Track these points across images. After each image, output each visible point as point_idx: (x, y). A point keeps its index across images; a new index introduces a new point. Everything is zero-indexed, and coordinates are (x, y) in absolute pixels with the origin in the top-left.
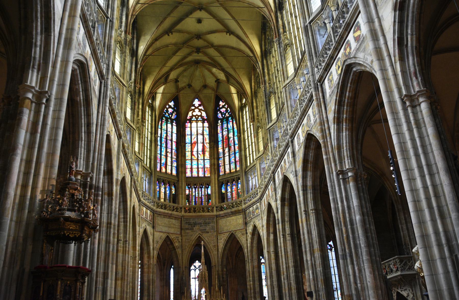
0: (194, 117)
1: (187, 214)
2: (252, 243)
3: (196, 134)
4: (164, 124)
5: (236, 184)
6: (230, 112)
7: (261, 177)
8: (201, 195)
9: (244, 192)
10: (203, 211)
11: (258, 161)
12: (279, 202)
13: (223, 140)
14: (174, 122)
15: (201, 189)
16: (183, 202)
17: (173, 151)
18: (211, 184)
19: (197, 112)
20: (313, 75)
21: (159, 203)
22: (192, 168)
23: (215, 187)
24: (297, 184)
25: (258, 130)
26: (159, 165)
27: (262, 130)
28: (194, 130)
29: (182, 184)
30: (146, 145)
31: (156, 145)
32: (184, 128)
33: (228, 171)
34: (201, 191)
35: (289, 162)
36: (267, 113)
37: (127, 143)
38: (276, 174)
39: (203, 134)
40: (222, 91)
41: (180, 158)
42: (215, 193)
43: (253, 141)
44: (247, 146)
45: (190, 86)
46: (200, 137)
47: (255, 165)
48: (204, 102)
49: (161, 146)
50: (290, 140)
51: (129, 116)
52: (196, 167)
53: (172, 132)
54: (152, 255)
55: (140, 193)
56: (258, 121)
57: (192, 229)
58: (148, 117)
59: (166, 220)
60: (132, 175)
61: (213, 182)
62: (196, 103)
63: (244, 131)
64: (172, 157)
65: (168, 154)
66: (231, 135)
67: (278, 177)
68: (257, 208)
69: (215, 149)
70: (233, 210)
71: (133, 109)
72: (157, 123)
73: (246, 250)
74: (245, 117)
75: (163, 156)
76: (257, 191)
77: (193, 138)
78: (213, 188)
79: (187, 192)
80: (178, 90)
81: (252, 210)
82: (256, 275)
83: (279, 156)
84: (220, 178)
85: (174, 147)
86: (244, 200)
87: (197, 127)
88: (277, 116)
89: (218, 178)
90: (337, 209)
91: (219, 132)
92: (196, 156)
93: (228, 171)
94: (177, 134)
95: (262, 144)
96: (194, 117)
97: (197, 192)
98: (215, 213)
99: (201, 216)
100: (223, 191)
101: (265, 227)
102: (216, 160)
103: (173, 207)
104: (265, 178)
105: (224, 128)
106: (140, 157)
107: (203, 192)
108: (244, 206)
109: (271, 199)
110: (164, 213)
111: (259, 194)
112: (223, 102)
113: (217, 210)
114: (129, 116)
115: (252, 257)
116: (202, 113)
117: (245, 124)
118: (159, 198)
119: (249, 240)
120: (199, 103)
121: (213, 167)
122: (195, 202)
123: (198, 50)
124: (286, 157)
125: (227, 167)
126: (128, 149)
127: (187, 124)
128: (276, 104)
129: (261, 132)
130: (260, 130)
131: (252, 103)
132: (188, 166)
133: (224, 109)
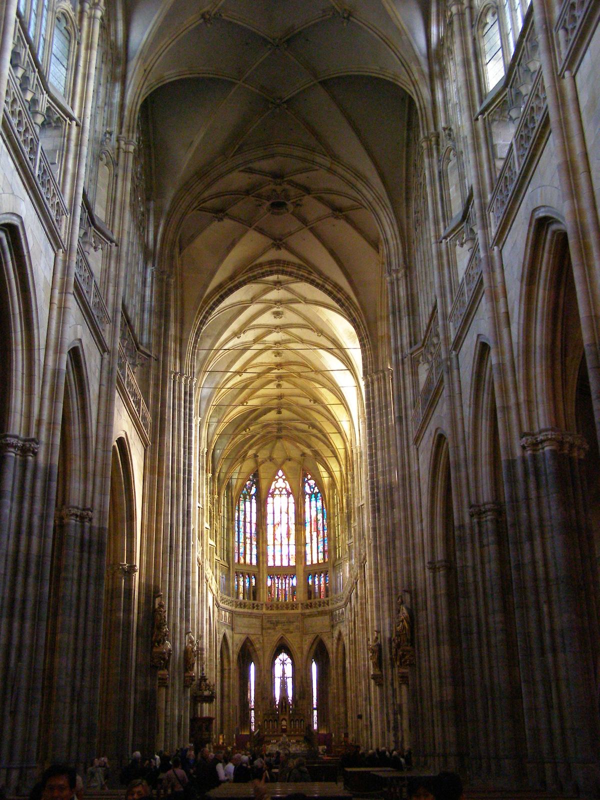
0: (277, 490)
1: (269, 612)
2: (337, 648)
10: (287, 608)
14: (254, 497)
16: (264, 597)
20: (360, 554)
22: (274, 556)
29: (263, 575)
39: (288, 513)
40: (309, 465)
41: (261, 544)
45: (271, 459)
46: (284, 516)
48: (289, 475)
52: (280, 554)
53: (251, 512)
54: (231, 659)
57: (274, 629)
58: (224, 501)
59: (246, 620)
63: (334, 516)
64: (251, 544)
70: (320, 609)
73: (331, 655)
75: (241, 544)
79: (269, 583)
80: (258, 465)
82: (341, 683)
90: (364, 665)
98: (299, 611)
99: (284, 614)
100: (310, 582)
101: (348, 637)
108: (331, 607)
110: (244, 612)
115: (337, 662)
119: (335, 645)
123: (280, 430)
133: (312, 482)
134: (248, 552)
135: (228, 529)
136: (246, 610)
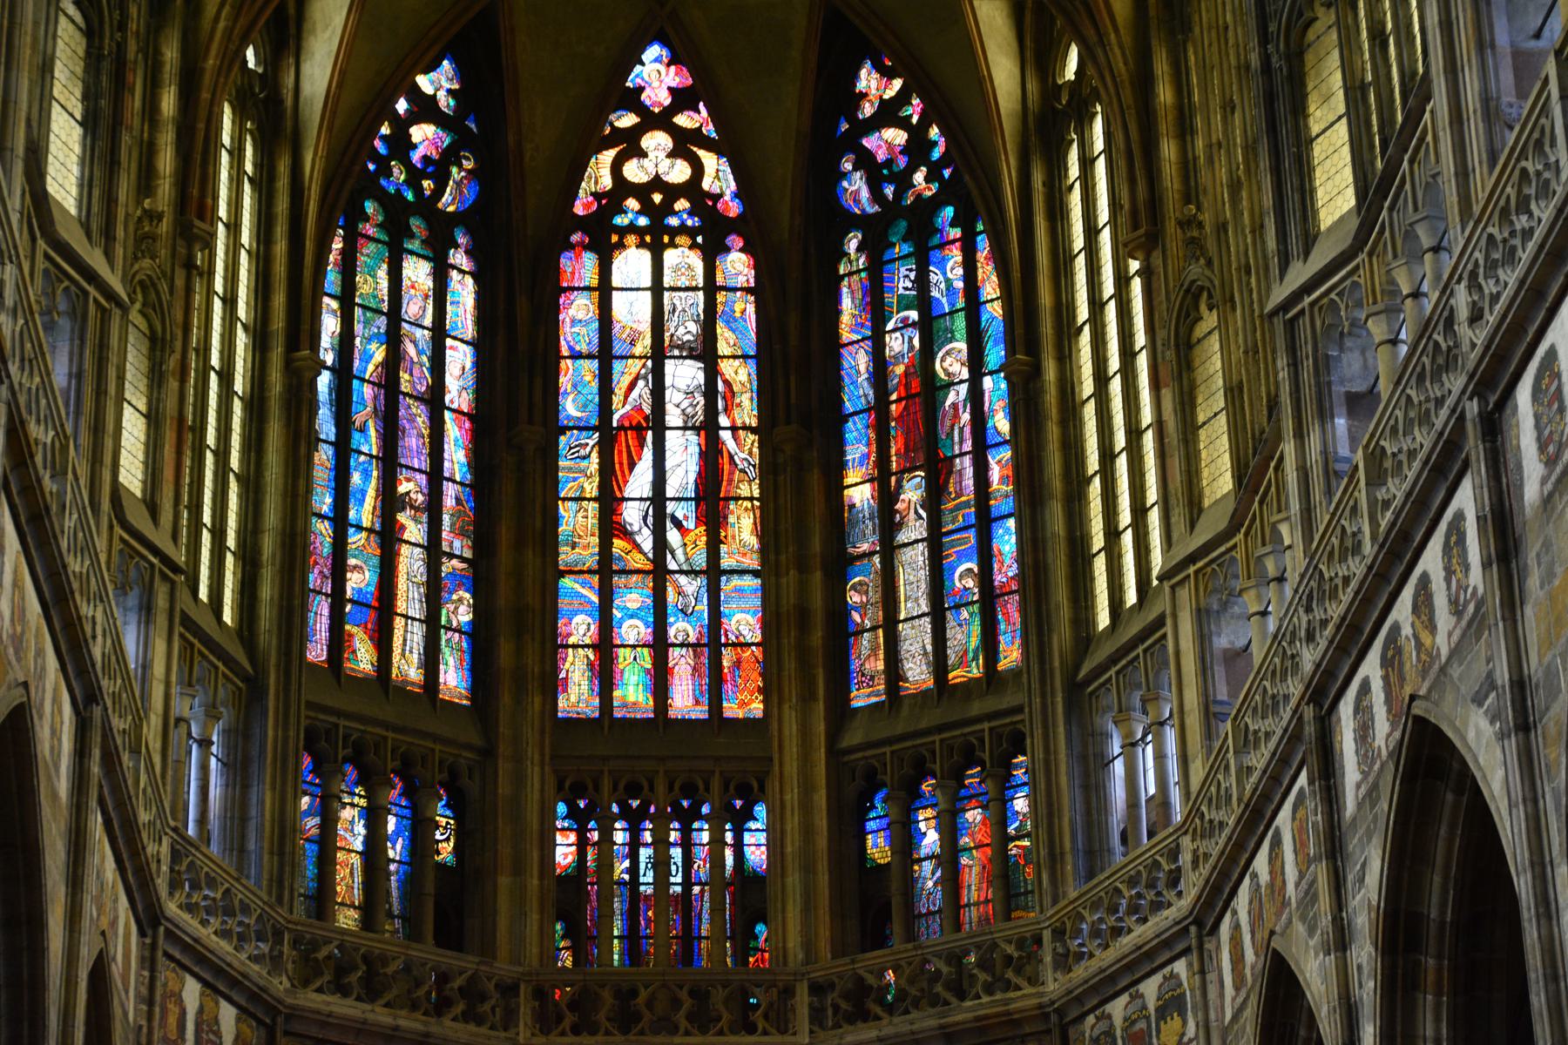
0: (632, 204)
3: (644, 345)
4: (370, 255)
5: (989, 786)
6: (945, 160)
7: (1209, 735)
8: (687, 883)
9: (1055, 858)
11: (1184, 594)
12: (1364, 953)
13: (879, 410)
14: (462, 239)
15: (686, 832)
17: (450, 492)
18: (773, 786)
19: (657, 159)
21: (315, 945)
23: (806, 807)
24: (1533, 798)
25: (1189, 317)
26: (320, 612)
27: (1223, 326)
28: (632, 311)
29: (519, 779)
30: (211, 439)
31: (301, 440)
32: (550, 294)
33: (917, 672)
34: (687, 844)
35: (1457, 609)
36: (1276, 170)
37: (50, 419)
38: (1346, 708)
39: (705, 352)
41: (504, 557)
42: (808, 869)
43: (1147, 417)
44: (1093, 463)
46: (684, 375)
47: (1160, 622)
49: (343, 449)
50: (1472, 408)
51: (64, 181)
53: (439, 332)
55: (159, 850)
56: (1195, 247)
58: (233, 198)
60: (86, 697)
61: (791, 767)
62: (656, 75)
63: (1066, 331)
64: (433, 550)
65: (402, 518)
66: (952, 362)
67: (1364, 732)
68: (1172, 1004)
69: (815, 480)
71: (100, 126)
72: (309, 245)
74: (1075, 198)
75: (355, 539)
76: (1174, 854)
77: (621, 382)
78: (793, 823)
81: (1129, 1022)
83: (1368, 548)
84: (854, 736)
85: (456, 457)
86: (1059, 934)
87: (657, 289)
88: (1361, 194)
89: (833, 735)
91: (846, 335)
92: (646, 541)
93: (917, 672)
94: (481, 345)
95: (1224, 442)
96: (632, 204)
97: (645, 854)
102: (818, 576)
103: (443, 978)
104: (1247, 741)
105: (890, 299)
106: (162, 540)
107: (701, 853)
108: (1054, 985)
109: (1300, 928)
111: (1193, 885)
112: (887, 74)
113: (817, 1017)
114: (64, 181)
116: (698, 169)
117: (1080, 262)
118: (322, 899)
120: (673, 77)
121: (789, 639)
122: (632, 937)
124: (1431, 560)
125: (916, 639)
126: (59, 473)
127: (566, 262)
128: (1355, 92)
129: (1214, 343)
130: (1210, 320)
131: (1144, 82)
132: (580, 627)
133: (896, 136)
134: (409, 599)
135: (256, 406)
136: (380, 1015)
